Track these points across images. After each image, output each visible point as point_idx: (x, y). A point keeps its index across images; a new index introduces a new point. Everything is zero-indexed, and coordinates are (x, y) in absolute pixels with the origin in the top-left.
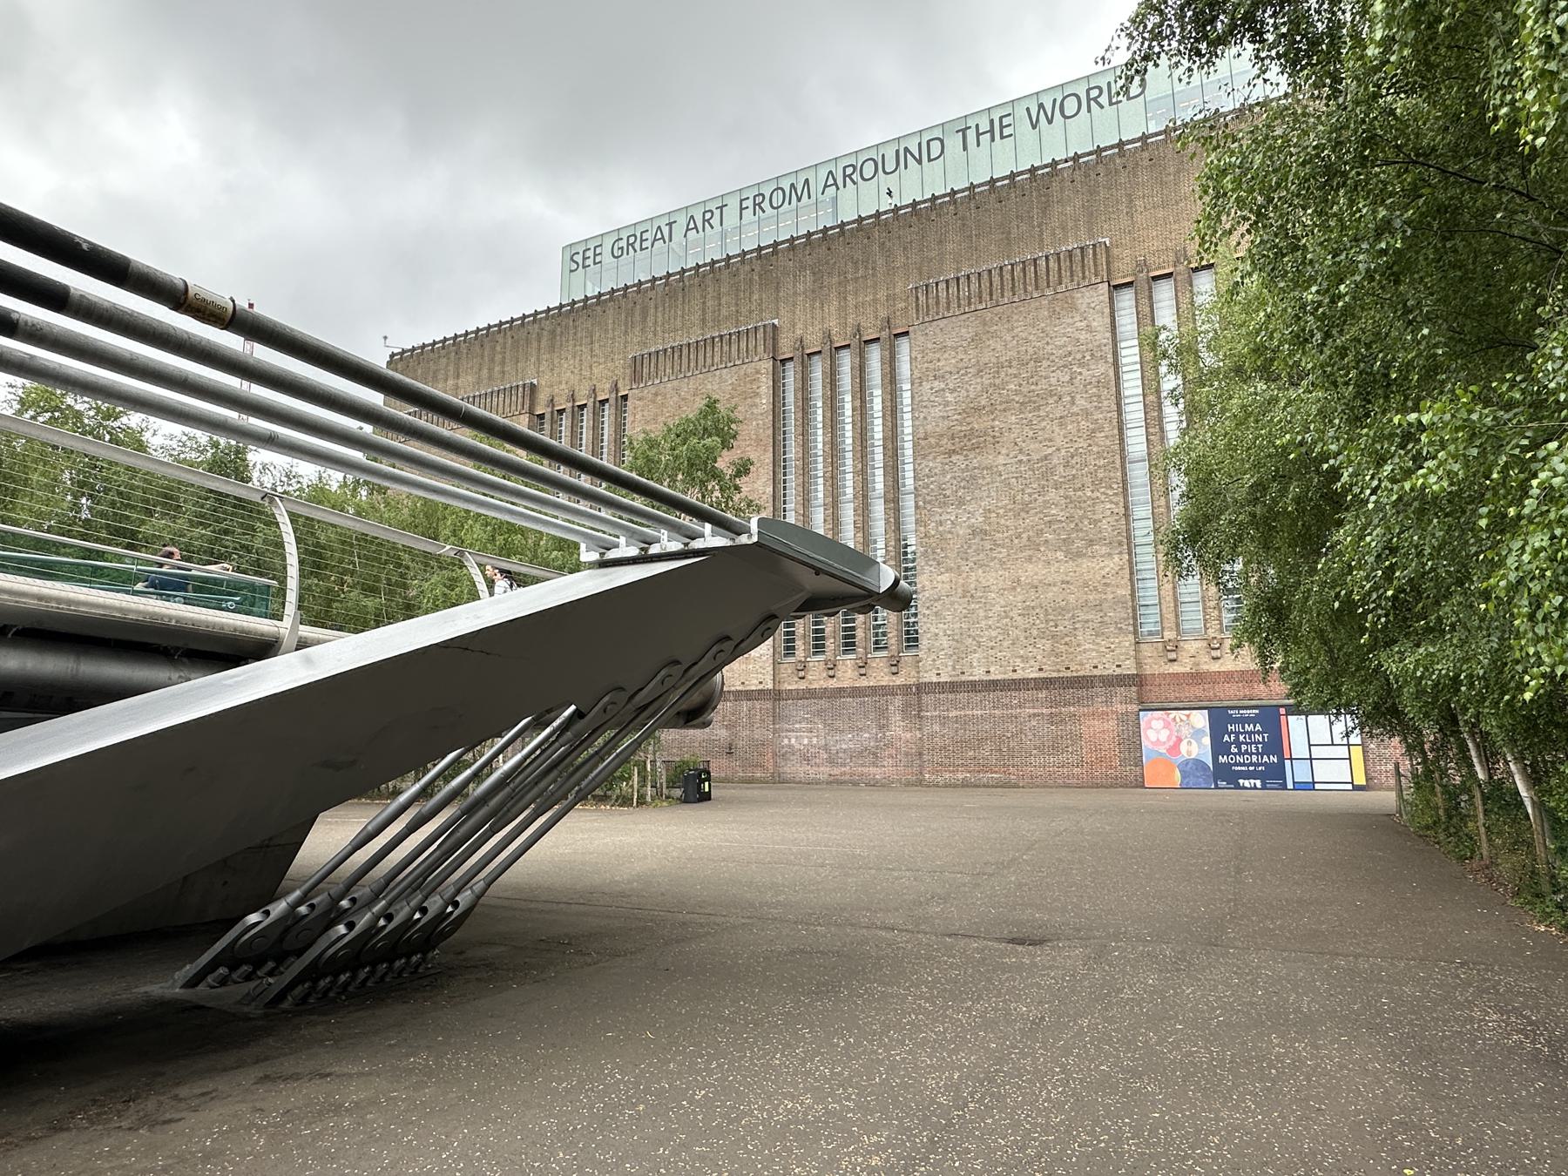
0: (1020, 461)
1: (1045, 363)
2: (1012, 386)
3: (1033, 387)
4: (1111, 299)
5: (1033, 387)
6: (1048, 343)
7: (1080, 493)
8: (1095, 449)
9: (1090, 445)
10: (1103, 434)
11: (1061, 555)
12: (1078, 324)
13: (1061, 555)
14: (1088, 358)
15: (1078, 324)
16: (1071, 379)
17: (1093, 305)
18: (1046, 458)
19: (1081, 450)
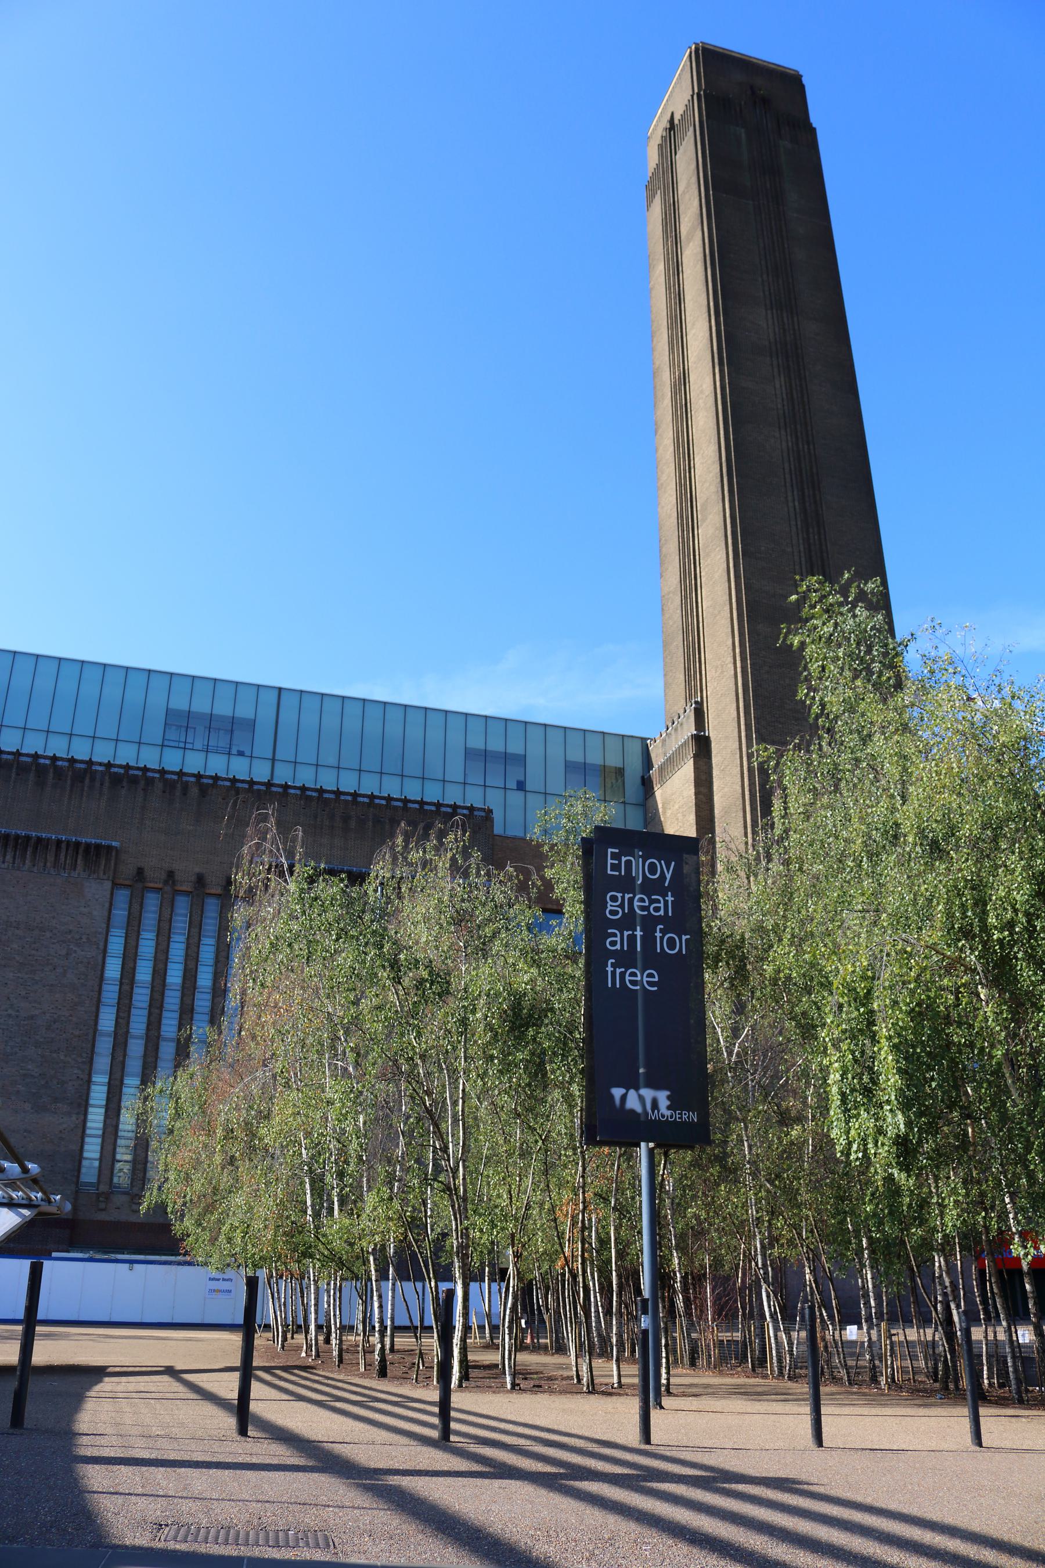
0: (10, 1016)
1: (48, 934)
2: (15, 946)
3: (33, 952)
4: (112, 894)
5: (33, 952)
6: (54, 918)
7: (54, 1055)
8: (74, 1019)
9: (71, 1016)
10: (83, 1009)
11: (27, 1106)
12: (82, 909)
13: (27, 1106)
14: (84, 940)
15: (82, 909)
16: (67, 954)
17: (97, 897)
18: (32, 1017)
19: (63, 1018)
